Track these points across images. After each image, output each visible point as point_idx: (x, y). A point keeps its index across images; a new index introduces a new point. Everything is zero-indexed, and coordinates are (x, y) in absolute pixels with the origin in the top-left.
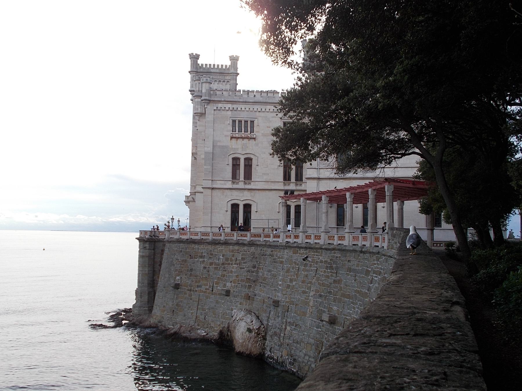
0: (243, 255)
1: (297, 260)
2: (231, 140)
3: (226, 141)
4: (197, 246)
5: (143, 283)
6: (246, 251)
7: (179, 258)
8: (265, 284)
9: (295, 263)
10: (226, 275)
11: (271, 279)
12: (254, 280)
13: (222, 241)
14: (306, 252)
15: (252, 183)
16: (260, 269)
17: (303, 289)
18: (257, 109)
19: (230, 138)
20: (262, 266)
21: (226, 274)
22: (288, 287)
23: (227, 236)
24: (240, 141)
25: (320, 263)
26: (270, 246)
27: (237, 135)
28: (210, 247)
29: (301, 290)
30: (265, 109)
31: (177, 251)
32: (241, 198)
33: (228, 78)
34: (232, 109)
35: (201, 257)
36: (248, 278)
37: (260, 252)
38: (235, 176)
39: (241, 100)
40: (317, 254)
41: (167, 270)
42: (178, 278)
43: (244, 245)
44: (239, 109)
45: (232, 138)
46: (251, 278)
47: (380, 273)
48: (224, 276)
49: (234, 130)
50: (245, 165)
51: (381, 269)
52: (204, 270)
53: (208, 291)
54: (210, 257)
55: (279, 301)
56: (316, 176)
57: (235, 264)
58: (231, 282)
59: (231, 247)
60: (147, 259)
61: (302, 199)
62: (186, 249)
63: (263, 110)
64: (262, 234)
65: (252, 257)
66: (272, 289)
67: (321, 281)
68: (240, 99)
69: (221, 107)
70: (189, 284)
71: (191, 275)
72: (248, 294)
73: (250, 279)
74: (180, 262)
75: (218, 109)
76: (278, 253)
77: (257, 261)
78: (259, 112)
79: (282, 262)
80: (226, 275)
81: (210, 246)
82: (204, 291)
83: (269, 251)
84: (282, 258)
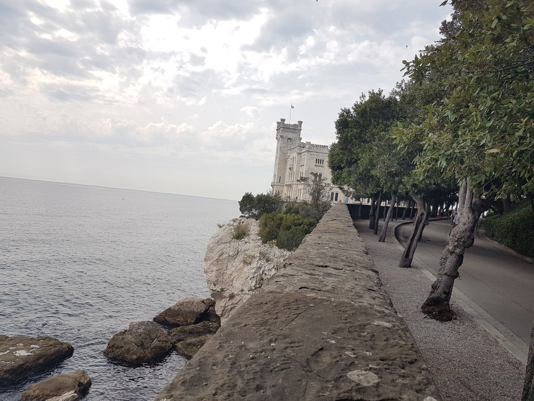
3: (313, 167)
24: (318, 167)
33: (297, 131)
45: (315, 166)
49: (316, 163)
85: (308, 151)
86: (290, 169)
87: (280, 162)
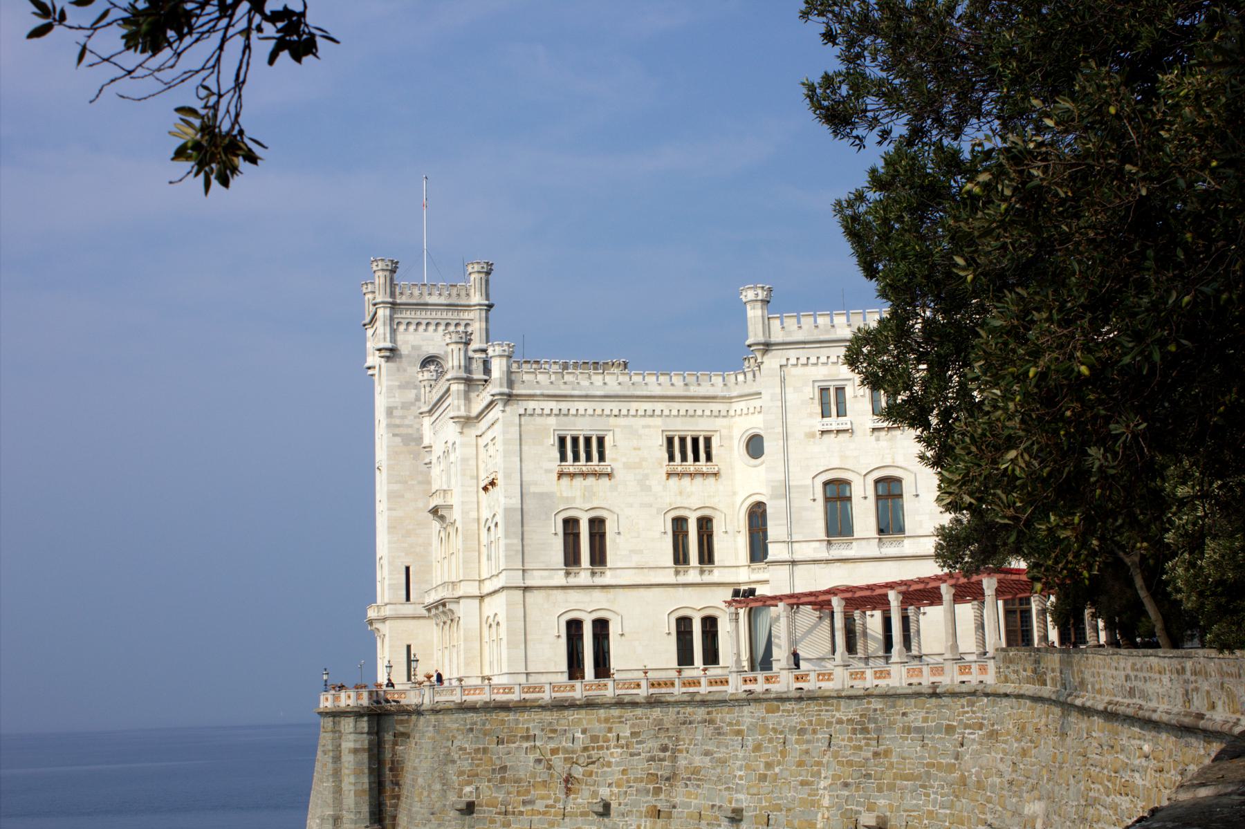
0: (633, 726)
1: (779, 723)
2: (559, 479)
4: (512, 716)
5: (360, 812)
6: (641, 719)
7: (467, 746)
8: (699, 780)
9: (775, 730)
10: (597, 773)
11: (714, 769)
12: (668, 775)
13: (579, 700)
14: (798, 706)
15: (608, 573)
16: (680, 751)
17: (801, 778)
18: (611, 410)
19: (556, 476)
20: (686, 746)
21: (596, 770)
22: (763, 778)
23: (589, 690)
24: (578, 481)
25: (837, 723)
26: (703, 703)
27: (571, 467)
28: (547, 716)
29: (797, 781)
30: (628, 410)
31: (458, 730)
32: (587, 607)
33: (466, 316)
34: (558, 412)
35: (527, 738)
36: (651, 774)
37: (675, 717)
38: (572, 558)
39: (576, 393)
40: (827, 708)
41: (437, 774)
42: (468, 789)
43: (634, 704)
44: (573, 411)
45: (561, 475)
46: (659, 773)
47: (981, 727)
48: (591, 775)
49: (563, 458)
50: (592, 536)
51: (983, 718)
52: (536, 767)
53: (553, 810)
54: (549, 738)
55: (742, 810)
56: (786, 556)
57: (617, 747)
58: (610, 785)
59: (602, 711)
60: (366, 756)
61: (781, 605)
62: (484, 724)
63: (624, 412)
64: (677, 680)
65: (657, 728)
66: (718, 788)
67: (843, 757)
68: (573, 389)
69: (534, 409)
70: (500, 799)
71: (503, 780)
72: (655, 806)
73: (657, 775)
74: (469, 753)
75: (528, 412)
76: (723, 716)
77: (669, 737)
78: (616, 416)
79: (739, 733)
80: (597, 773)
81: (549, 713)
82: (541, 810)
83: (701, 713)
84: (738, 723)
85: (509, 398)
86: (435, 511)
87: (396, 487)
